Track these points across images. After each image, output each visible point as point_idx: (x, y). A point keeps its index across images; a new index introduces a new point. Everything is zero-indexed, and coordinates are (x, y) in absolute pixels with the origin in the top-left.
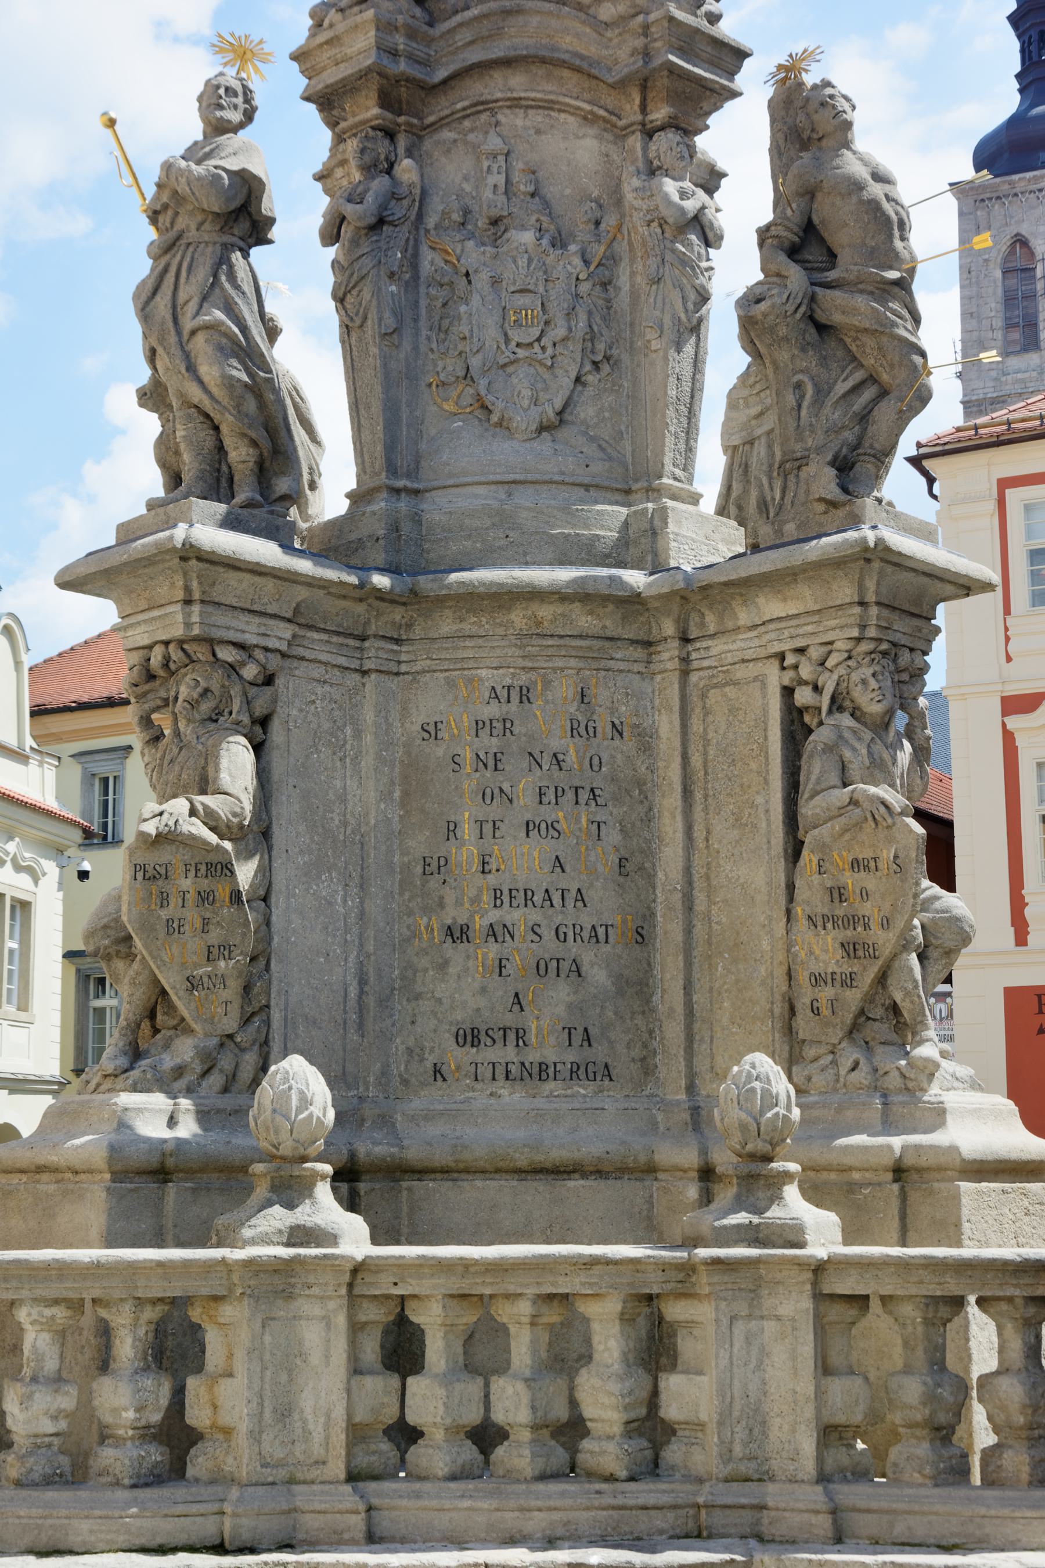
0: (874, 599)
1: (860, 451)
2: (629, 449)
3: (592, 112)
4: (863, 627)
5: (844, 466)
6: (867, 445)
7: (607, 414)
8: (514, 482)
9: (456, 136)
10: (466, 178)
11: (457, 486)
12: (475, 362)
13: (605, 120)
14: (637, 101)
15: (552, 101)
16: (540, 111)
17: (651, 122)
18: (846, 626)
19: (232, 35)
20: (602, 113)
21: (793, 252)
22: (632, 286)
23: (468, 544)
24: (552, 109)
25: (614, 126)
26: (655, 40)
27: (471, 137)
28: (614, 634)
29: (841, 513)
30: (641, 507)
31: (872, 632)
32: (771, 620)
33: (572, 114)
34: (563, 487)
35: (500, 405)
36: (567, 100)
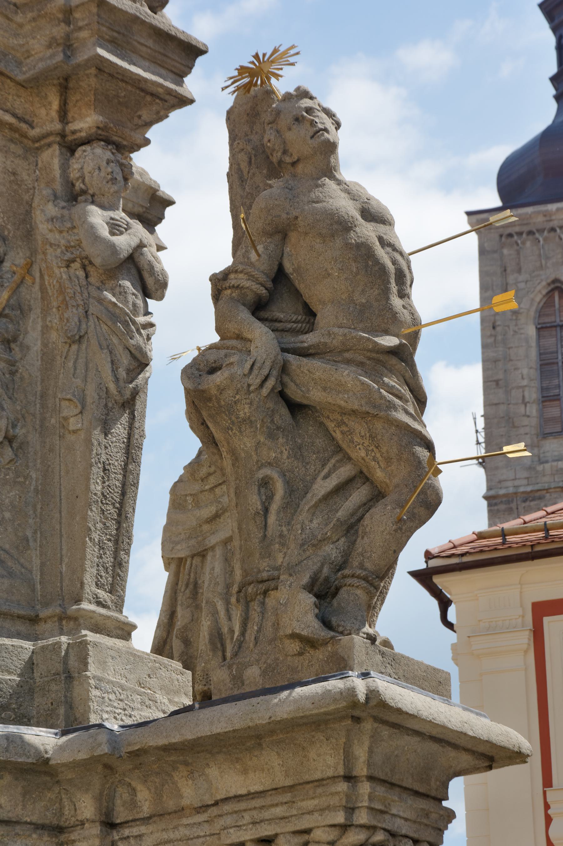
0: (365, 772)
1: (346, 572)
2: (36, 562)
4: (350, 810)
5: (324, 592)
6: (356, 564)
7: (7, 515)
13: (11, 127)
14: (55, 105)
17: (74, 132)
18: (328, 808)
21: (258, 308)
22: (45, 345)
25: (24, 135)
26: (80, 29)
28: (11, 816)
29: (320, 654)
30: (51, 641)
31: (362, 817)
32: (226, 800)
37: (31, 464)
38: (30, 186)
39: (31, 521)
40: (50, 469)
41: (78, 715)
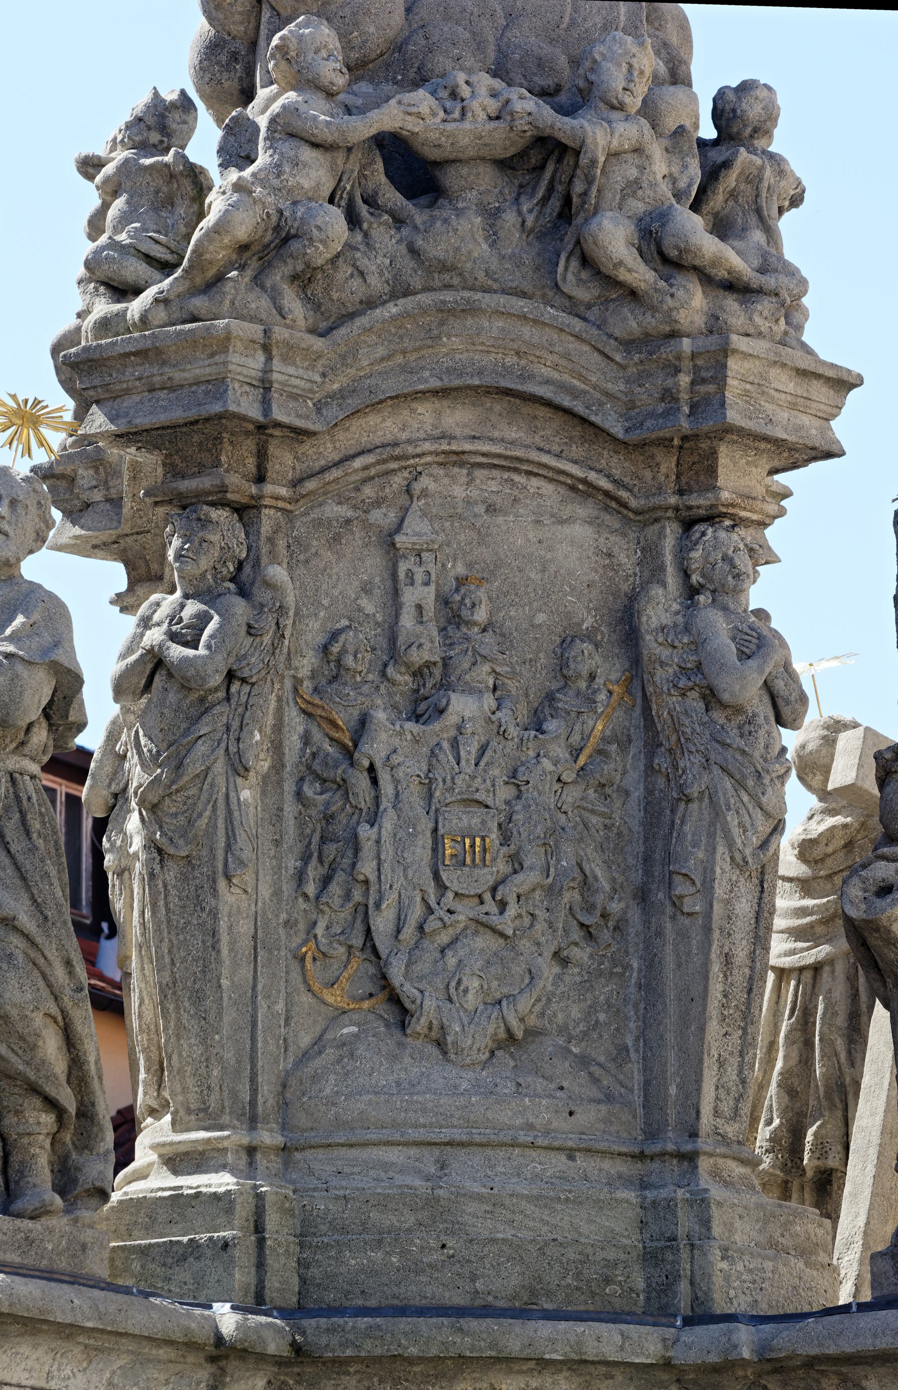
3: (584, 481)
7: (602, 1017)
8: (449, 1144)
9: (350, 514)
10: (366, 589)
13: (607, 494)
16: (495, 473)
17: (690, 508)
19: (14, 397)
20: (604, 483)
22: (649, 792)
23: (377, 1256)
24: (516, 470)
25: (625, 505)
26: (704, 381)
27: (376, 516)
30: (664, 1193)
33: (551, 480)
35: (430, 1004)
36: (545, 459)
37: (631, 950)
38: (630, 572)
39: (632, 1025)
40: (657, 959)
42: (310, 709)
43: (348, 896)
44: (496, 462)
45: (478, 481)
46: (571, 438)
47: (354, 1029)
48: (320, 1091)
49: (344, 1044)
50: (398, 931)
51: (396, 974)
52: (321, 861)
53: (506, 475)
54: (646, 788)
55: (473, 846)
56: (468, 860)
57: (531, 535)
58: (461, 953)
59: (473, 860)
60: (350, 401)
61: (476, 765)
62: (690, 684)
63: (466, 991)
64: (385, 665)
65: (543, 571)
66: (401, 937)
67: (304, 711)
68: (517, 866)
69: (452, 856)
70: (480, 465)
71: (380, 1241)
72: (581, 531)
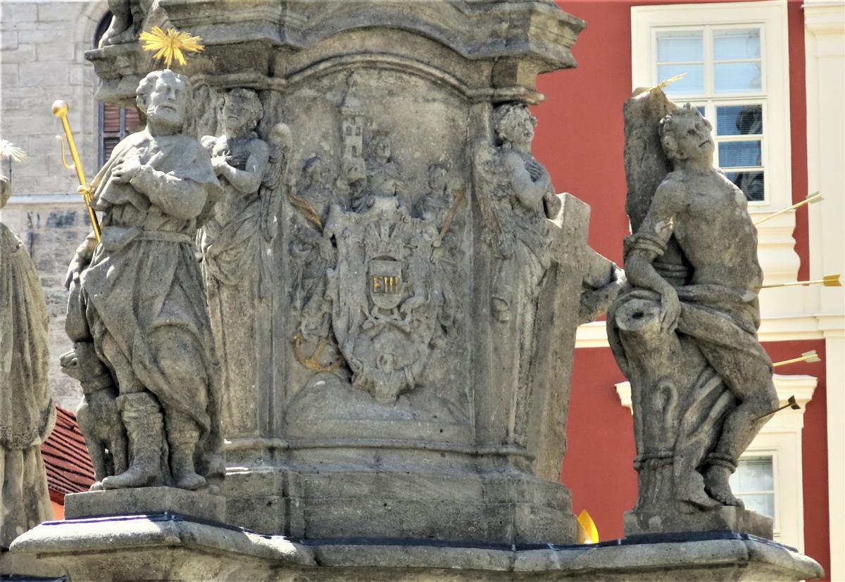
1: (717, 455)
2: (472, 412)
3: (442, 79)
6: (723, 450)
7: (452, 377)
8: (382, 447)
10: (324, 137)
11: (327, 448)
12: (340, 325)
13: (453, 87)
15: (407, 66)
16: (393, 73)
17: (500, 96)
20: (453, 81)
22: (477, 253)
24: (404, 72)
25: (463, 93)
26: (515, 27)
27: (329, 96)
33: (422, 78)
34: (424, 453)
35: (366, 369)
36: (422, 66)
37: (467, 340)
39: (468, 382)
41: (519, 532)
42: (296, 204)
43: (319, 308)
44: (394, 67)
45: (384, 77)
46: (434, 55)
47: (322, 382)
48: (307, 416)
49: (318, 391)
50: (349, 328)
51: (348, 352)
52: (303, 288)
53: (398, 74)
54: (474, 251)
55: (388, 282)
56: (386, 291)
57: (412, 108)
58: (383, 341)
59: (389, 290)
60: (321, 32)
61: (390, 236)
62: (505, 194)
63: (386, 362)
64: (336, 180)
65: (419, 128)
66: (350, 332)
67: (293, 205)
68: (411, 293)
69: (378, 287)
70: (386, 69)
71: (351, 501)
72: (438, 107)
